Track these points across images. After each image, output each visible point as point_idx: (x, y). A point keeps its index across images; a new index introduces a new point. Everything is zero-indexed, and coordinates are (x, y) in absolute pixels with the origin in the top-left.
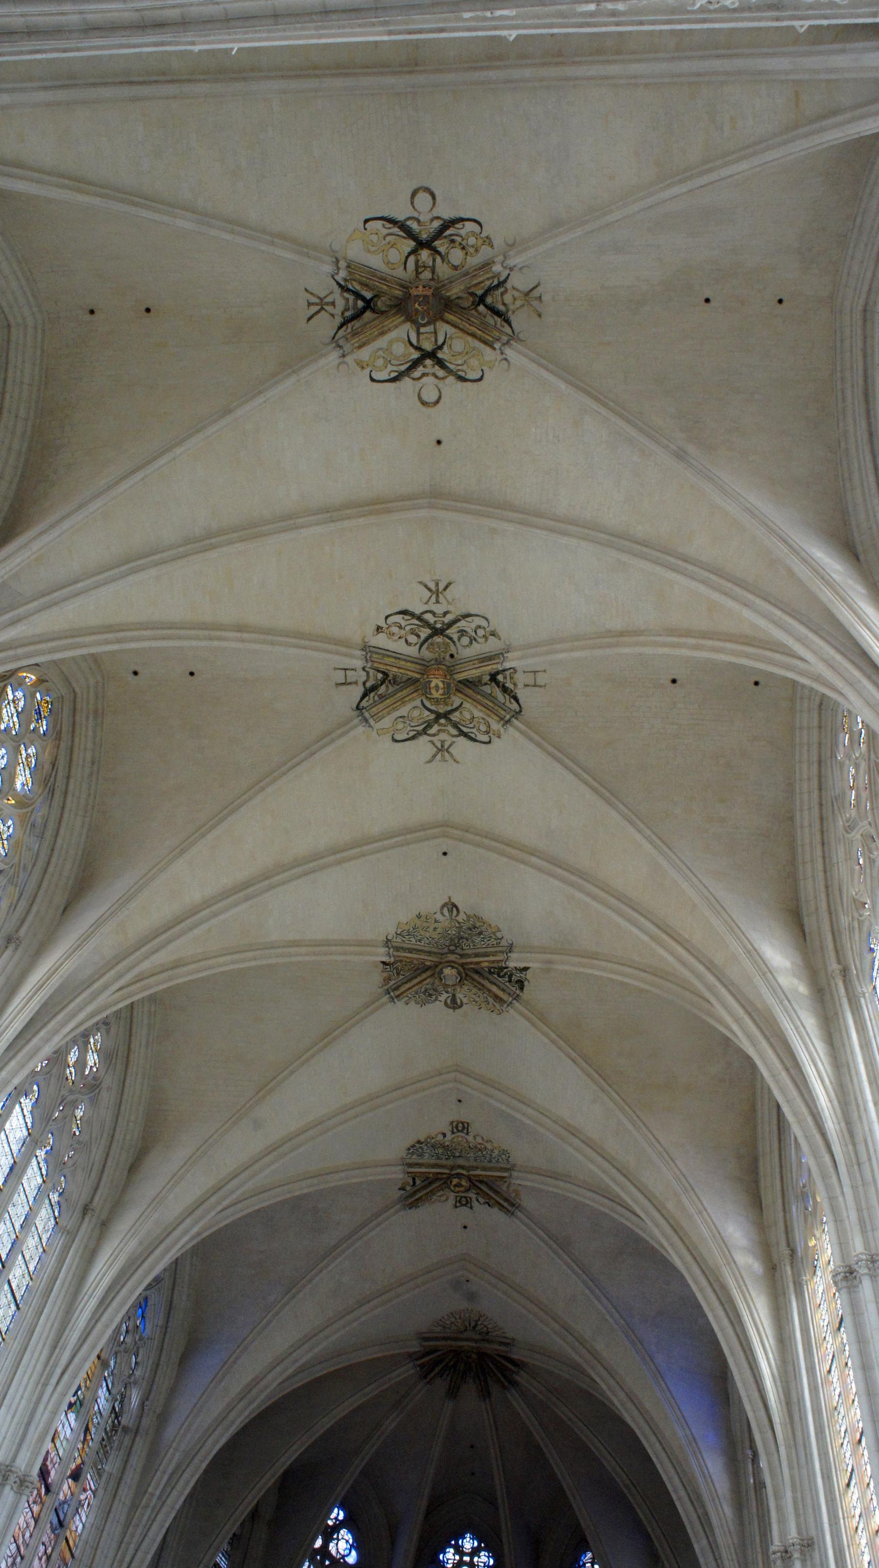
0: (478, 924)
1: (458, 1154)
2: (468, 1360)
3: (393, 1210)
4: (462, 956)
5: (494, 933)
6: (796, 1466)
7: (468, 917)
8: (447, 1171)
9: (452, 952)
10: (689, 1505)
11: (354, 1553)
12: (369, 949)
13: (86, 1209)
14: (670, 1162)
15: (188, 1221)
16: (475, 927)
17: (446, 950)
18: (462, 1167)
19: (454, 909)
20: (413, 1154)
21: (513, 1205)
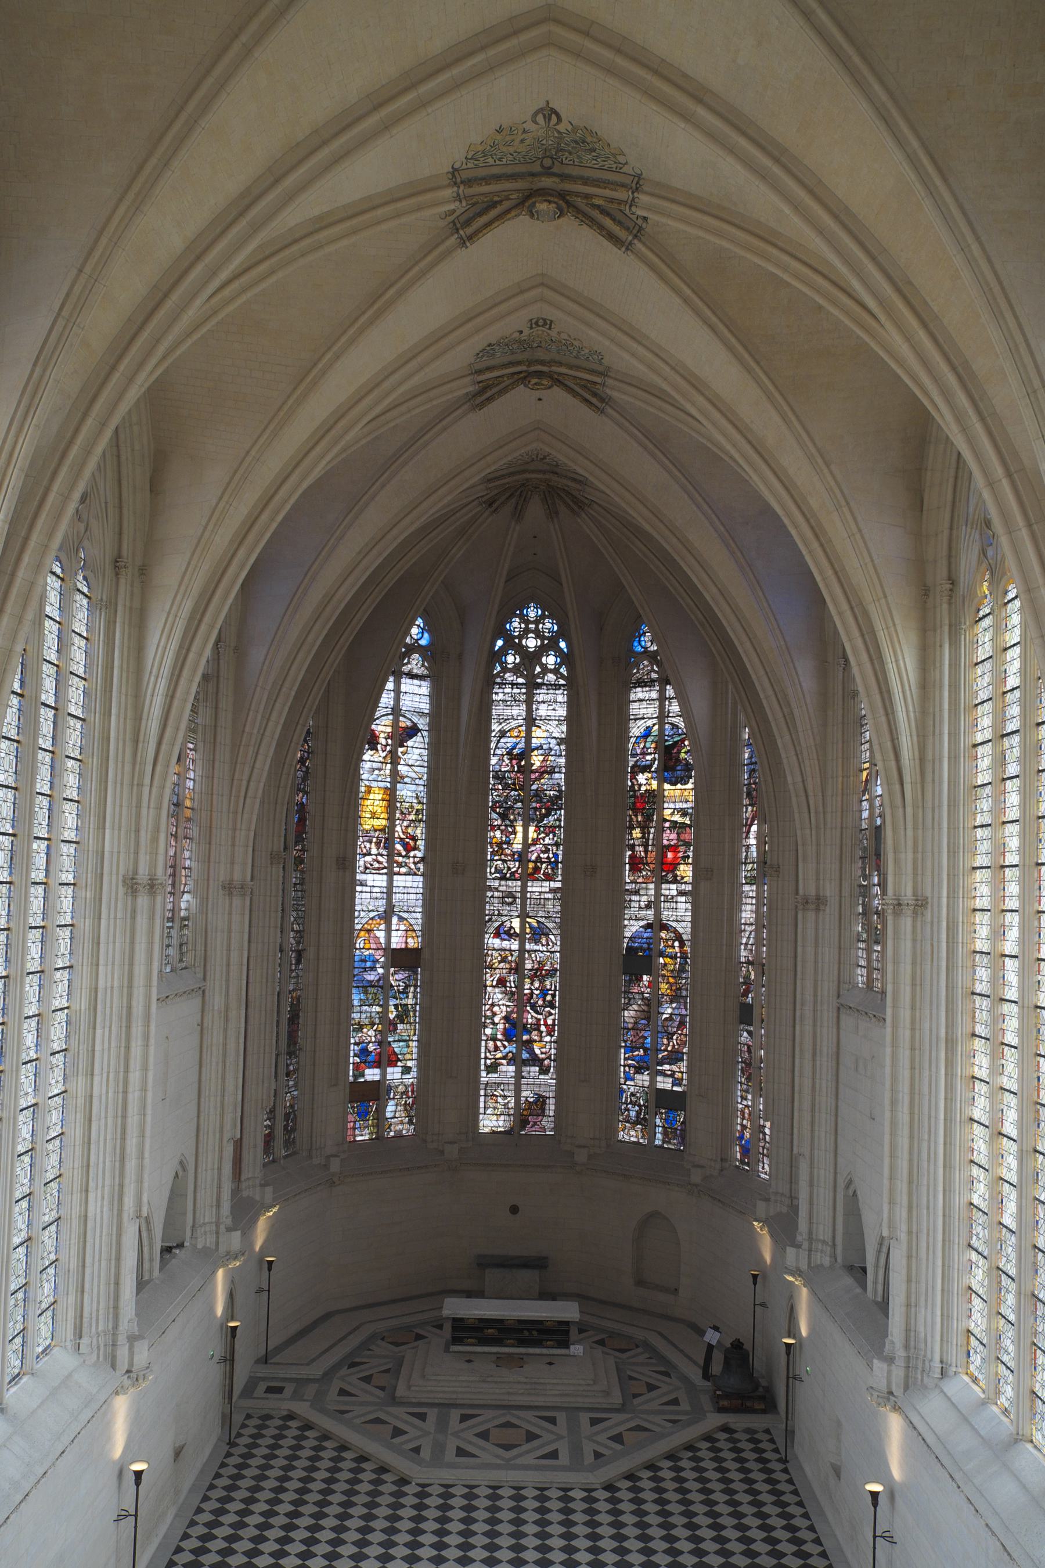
0: (589, 139)
1: (536, 345)
2: (536, 490)
3: (460, 411)
4: (564, 177)
5: (614, 155)
7: (575, 129)
8: (524, 368)
9: (548, 172)
11: (426, 635)
12: (428, 197)
13: (117, 563)
14: (824, 467)
16: (584, 142)
17: (537, 168)
18: (542, 363)
19: (554, 118)
20: (483, 356)
21: (602, 400)
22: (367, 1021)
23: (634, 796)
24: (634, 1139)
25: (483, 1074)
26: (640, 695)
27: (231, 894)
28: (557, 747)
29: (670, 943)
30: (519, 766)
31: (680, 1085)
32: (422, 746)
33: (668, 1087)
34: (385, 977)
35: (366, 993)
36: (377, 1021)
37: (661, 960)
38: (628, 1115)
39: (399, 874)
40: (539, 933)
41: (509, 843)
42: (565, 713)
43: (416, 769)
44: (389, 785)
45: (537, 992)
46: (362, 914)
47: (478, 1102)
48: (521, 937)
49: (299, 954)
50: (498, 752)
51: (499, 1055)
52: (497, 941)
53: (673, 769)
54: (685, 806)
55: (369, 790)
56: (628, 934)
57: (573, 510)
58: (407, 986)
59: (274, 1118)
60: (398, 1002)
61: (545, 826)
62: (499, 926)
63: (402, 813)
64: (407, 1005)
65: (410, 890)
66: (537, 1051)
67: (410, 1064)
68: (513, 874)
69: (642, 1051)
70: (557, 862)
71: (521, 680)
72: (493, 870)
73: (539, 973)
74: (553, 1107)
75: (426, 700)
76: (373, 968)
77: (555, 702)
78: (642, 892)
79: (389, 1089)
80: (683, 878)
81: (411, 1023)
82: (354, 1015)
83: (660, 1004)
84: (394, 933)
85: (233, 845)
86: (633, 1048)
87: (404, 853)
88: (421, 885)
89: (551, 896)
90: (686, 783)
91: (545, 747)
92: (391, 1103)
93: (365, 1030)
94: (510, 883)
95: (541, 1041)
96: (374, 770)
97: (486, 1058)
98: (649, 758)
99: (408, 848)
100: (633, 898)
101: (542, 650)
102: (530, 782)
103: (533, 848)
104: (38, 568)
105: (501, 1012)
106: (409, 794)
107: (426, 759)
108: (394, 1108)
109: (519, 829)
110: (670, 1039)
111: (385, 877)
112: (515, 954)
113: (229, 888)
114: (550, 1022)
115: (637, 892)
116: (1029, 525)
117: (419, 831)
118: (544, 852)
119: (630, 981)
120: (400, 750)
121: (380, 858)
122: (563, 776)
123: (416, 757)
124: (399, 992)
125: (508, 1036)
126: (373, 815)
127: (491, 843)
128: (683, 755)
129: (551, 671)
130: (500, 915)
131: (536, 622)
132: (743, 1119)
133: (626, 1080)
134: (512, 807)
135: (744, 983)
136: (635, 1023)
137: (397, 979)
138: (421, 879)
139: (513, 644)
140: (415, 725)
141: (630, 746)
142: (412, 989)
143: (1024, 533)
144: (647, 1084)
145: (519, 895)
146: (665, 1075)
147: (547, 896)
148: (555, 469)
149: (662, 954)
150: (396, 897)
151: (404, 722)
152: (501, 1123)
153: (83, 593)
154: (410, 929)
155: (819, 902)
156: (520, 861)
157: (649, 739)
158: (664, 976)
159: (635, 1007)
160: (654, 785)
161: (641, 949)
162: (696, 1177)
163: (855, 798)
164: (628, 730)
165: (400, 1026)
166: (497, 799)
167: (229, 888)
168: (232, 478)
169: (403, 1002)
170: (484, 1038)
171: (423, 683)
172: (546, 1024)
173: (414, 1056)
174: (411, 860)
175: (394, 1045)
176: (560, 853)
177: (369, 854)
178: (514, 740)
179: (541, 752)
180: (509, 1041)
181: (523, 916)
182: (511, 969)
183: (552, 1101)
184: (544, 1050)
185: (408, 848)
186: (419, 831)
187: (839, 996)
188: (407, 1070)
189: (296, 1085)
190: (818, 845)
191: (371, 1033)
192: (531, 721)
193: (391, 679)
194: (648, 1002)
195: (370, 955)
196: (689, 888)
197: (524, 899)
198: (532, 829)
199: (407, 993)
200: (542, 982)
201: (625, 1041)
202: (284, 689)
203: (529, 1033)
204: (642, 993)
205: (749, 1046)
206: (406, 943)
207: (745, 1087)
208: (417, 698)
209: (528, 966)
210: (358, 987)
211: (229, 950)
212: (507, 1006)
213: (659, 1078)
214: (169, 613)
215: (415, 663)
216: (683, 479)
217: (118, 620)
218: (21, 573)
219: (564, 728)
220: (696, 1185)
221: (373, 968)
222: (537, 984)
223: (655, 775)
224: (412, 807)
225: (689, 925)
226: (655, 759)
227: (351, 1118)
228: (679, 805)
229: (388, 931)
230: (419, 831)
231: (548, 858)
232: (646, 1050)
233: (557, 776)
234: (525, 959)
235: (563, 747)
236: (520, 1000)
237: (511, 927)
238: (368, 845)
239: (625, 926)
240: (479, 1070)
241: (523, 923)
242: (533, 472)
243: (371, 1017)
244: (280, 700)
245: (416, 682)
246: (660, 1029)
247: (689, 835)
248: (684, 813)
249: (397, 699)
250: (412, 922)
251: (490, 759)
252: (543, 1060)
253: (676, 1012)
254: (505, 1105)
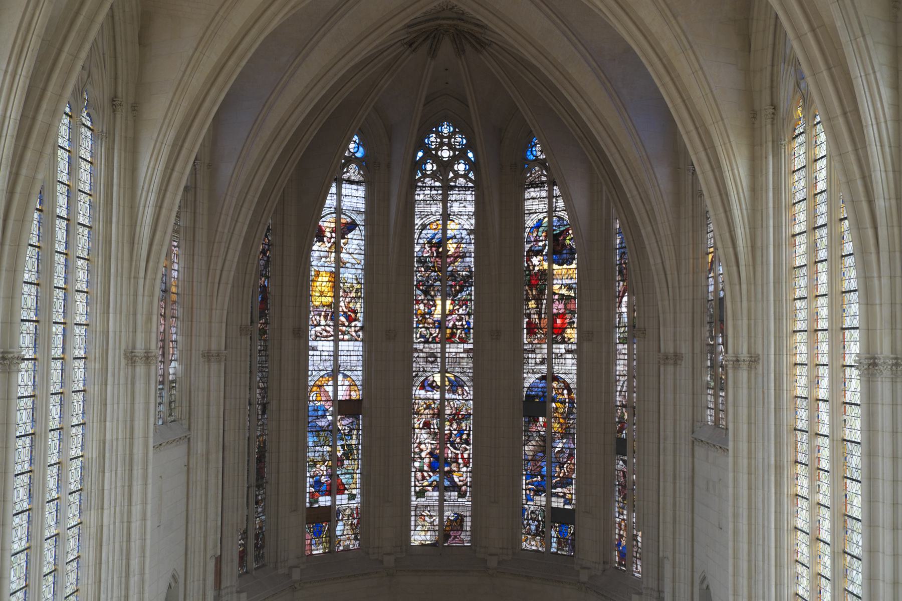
6: (753, 299)
10: (639, 201)
11: (361, 149)
13: (114, 102)
14: (672, 19)
15: (214, 91)
22: (319, 459)
23: (530, 275)
24: (534, 548)
25: (414, 498)
26: (533, 194)
27: (209, 361)
28: (467, 237)
29: (560, 391)
30: (438, 252)
31: (570, 504)
32: (360, 238)
33: (561, 505)
34: (333, 423)
35: (318, 436)
36: (328, 458)
37: (554, 405)
38: (530, 529)
39: (343, 340)
40: (456, 385)
41: (430, 314)
42: (473, 210)
43: (355, 256)
44: (333, 270)
45: (455, 432)
46: (314, 373)
47: (410, 521)
48: (441, 388)
49: (264, 407)
50: (421, 241)
51: (426, 483)
52: (422, 392)
53: (561, 253)
54: (570, 282)
55: (318, 274)
56: (527, 385)
57: (476, 49)
58: (351, 430)
59: (247, 538)
60: (344, 442)
61: (459, 300)
62: (424, 380)
63: (345, 292)
64: (351, 445)
65: (352, 353)
66: (456, 480)
67: (354, 492)
68: (434, 338)
69: (539, 478)
70: (469, 328)
71: (437, 184)
72: (418, 336)
73: (456, 417)
74: (469, 524)
75: (362, 201)
76: (324, 416)
77: (465, 201)
78: (537, 351)
79: (338, 512)
80: (569, 339)
82: (309, 454)
83: (553, 440)
84: (340, 388)
85: (210, 322)
86: (533, 476)
87: (347, 324)
88: (361, 349)
89: (464, 355)
90: (571, 264)
91: (458, 236)
92: (340, 523)
93: (318, 466)
94: (432, 346)
95: (459, 471)
96: (321, 258)
97: (415, 486)
98: (541, 244)
99: (350, 320)
100: (530, 356)
101: (454, 160)
102: (445, 265)
103: (450, 318)
104: (54, 113)
105: (426, 448)
106: (350, 276)
107: (363, 248)
108: (342, 528)
109: (439, 303)
110: (561, 467)
111: (332, 343)
112: (438, 402)
113: (208, 356)
114: (466, 456)
115: (533, 351)
116: (829, 69)
117: (358, 306)
118: (458, 320)
119: (529, 422)
120: (342, 241)
121: (328, 328)
122: (472, 259)
123: (354, 247)
124: (345, 435)
125: (433, 468)
126: (322, 294)
127: (416, 314)
128: (568, 242)
129: (462, 176)
130: (424, 371)
131: (449, 137)
132: (620, 530)
133: (527, 500)
134: (432, 285)
135: (619, 422)
136: (534, 455)
137: (343, 424)
138: (361, 344)
139: (430, 155)
140: (354, 221)
141: (526, 235)
143: (825, 74)
144: (544, 503)
145: (439, 355)
146: (558, 496)
147: (461, 355)
148: (461, 17)
149: (554, 400)
150: (341, 359)
151: (345, 219)
152: (428, 537)
153: (87, 127)
154: (353, 384)
155: (677, 358)
156: (439, 328)
157: (541, 229)
158: (556, 417)
159: (534, 443)
160: (546, 265)
161: (537, 396)
162: (584, 577)
163: (704, 276)
164: (524, 222)
165: (346, 462)
166: (420, 279)
167: (208, 356)
168: (204, 34)
169: (349, 443)
170: (413, 470)
171: (359, 187)
172: (463, 458)
173: (358, 486)
174: (353, 329)
175: (342, 477)
176: (471, 321)
177: (319, 325)
178: (433, 232)
179: (454, 241)
180: (434, 471)
181: (443, 372)
182: (434, 414)
183: (469, 519)
184: (461, 479)
185: (350, 320)
186: (359, 306)
187: (693, 433)
188: (352, 497)
189: (263, 511)
190: (675, 313)
191: (323, 468)
192: (446, 216)
193: (334, 185)
194: (543, 439)
195: (321, 406)
196: (574, 347)
197: (443, 358)
198: (448, 302)
199: (352, 435)
200: (459, 424)
201: (526, 470)
202: (249, 197)
203: (450, 465)
204: (539, 431)
205: (624, 472)
206: (350, 395)
207: (621, 504)
208: (355, 200)
209: (448, 412)
211: (208, 405)
212: (432, 444)
213: (553, 499)
214: (156, 141)
215: (353, 172)
216: (563, 25)
217: (116, 147)
218: (41, 117)
219: (473, 221)
220: (584, 583)
221: (324, 416)
222: (455, 426)
223: (546, 258)
224: (352, 287)
225: (575, 377)
226: (545, 245)
227: (308, 536)
228: (566, 282)
229: (335, 386)
230: (358, 306)
231: (462, 325)
232: (542, 477)
233: (468, 259)
234: (445, 406)
235: (472, 237)
236: (442, 439)
237: (434, 381)
238: (318, 318)
239: (525, 378)
240: (410, 496)
241: (443, 378)
242: (444, 19)
243: (323, 455)
244: (246, 205)
245: (354, 187)
246: (553, 460)
247: (574, 305)
248: (569, 287)
249: (339, 201)
250: (354, 378)
251: (414, 247)
252: (461, 486)
253: (566, 446)
254: (431, 523)
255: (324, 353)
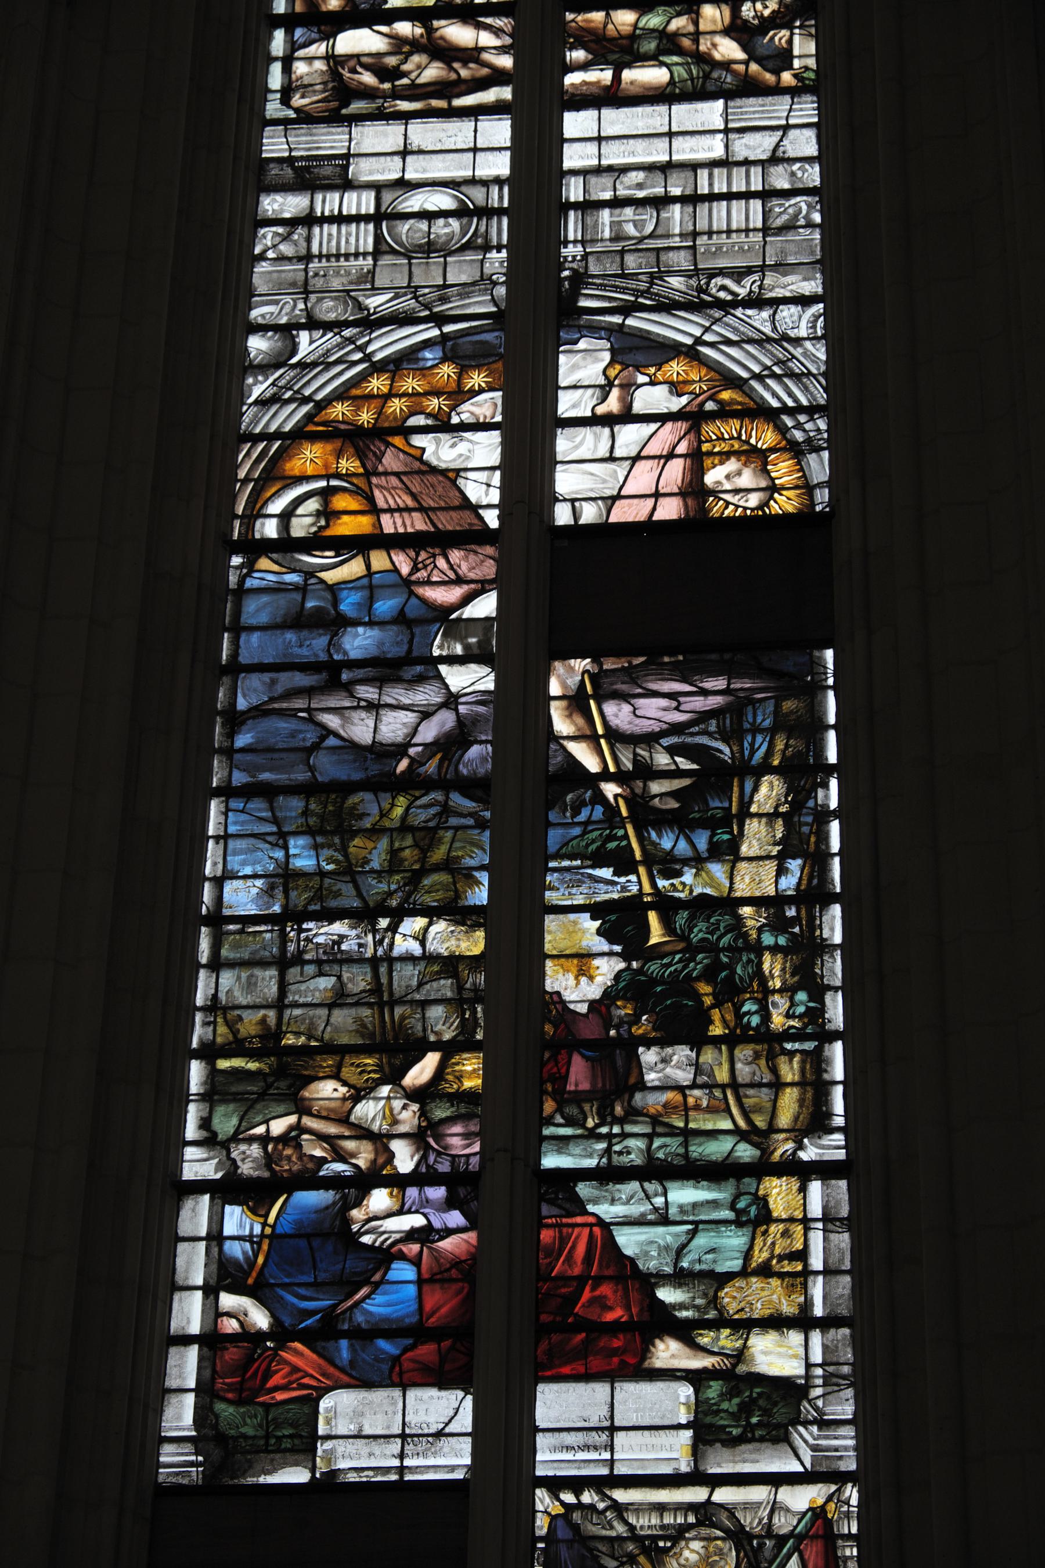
35: (333, 826)
39: (612, 97)
46: (306, 344)
81: (770, 1043)
88: (804, 143)
111: (499, 131)
124: (644, 814)
142: (769, 792)
154: (719, 407)
195: (370, 586)
210: (247, 792)
243: (380, 996)
250: (742, 361)
255: (415, 202)
